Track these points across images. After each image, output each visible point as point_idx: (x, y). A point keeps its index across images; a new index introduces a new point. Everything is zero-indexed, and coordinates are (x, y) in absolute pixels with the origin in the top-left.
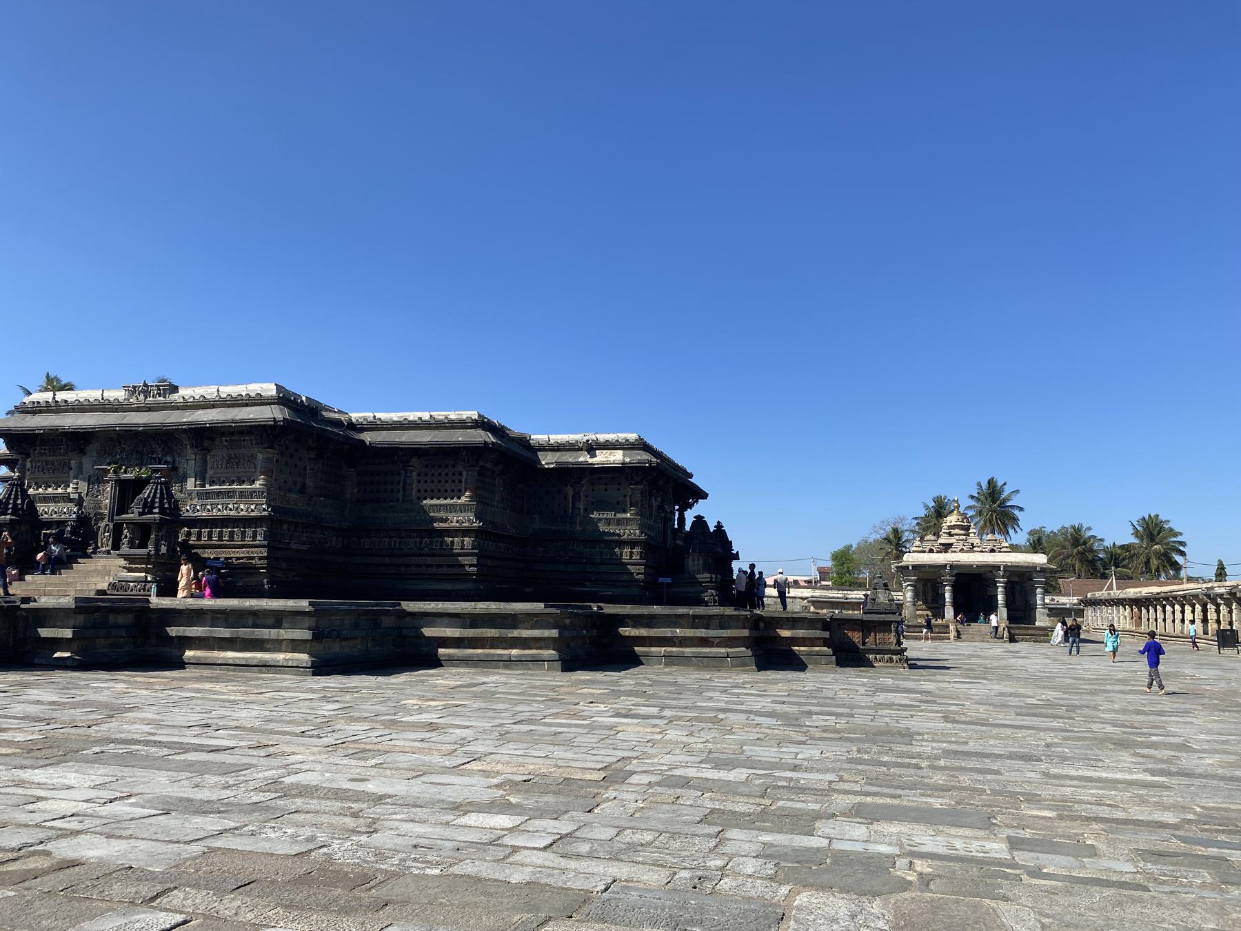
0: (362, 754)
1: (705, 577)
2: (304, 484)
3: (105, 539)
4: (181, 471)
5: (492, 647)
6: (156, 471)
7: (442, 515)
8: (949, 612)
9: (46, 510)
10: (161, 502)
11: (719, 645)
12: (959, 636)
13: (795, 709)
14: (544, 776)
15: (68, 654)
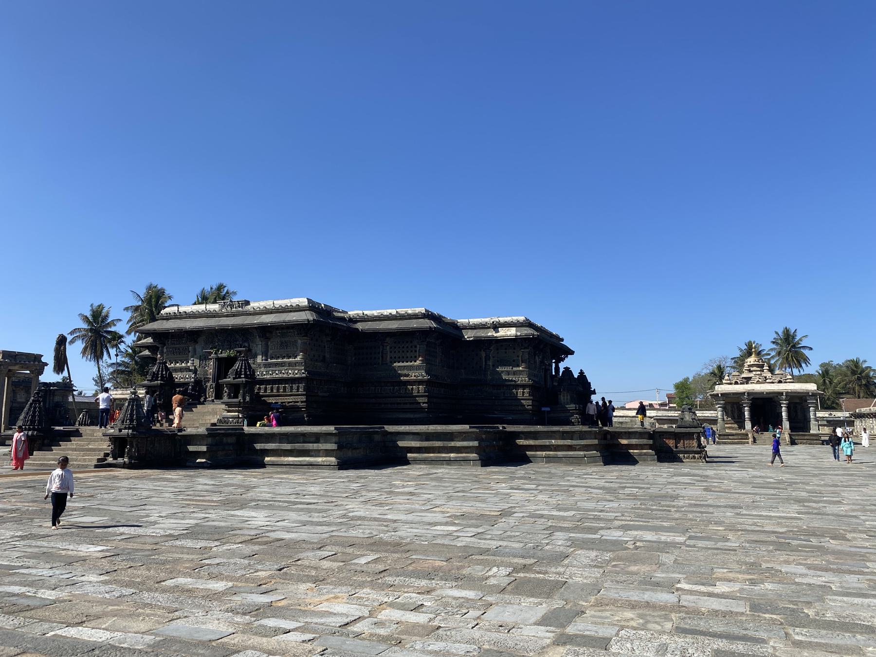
0: (381, 504)
1: (571, 406)
2: (324, 357)
3: (211, 393)
4: (253, 351)
5: (439, 452)
6: (238, 352)
7: (405, 372)
8: (748, 425)
9: (178, 377)
10: (245, 372)
11: (579, 450)
12: (755, 441)
13: (617, 485)
14: (470, 513)
15: (204, 460)
